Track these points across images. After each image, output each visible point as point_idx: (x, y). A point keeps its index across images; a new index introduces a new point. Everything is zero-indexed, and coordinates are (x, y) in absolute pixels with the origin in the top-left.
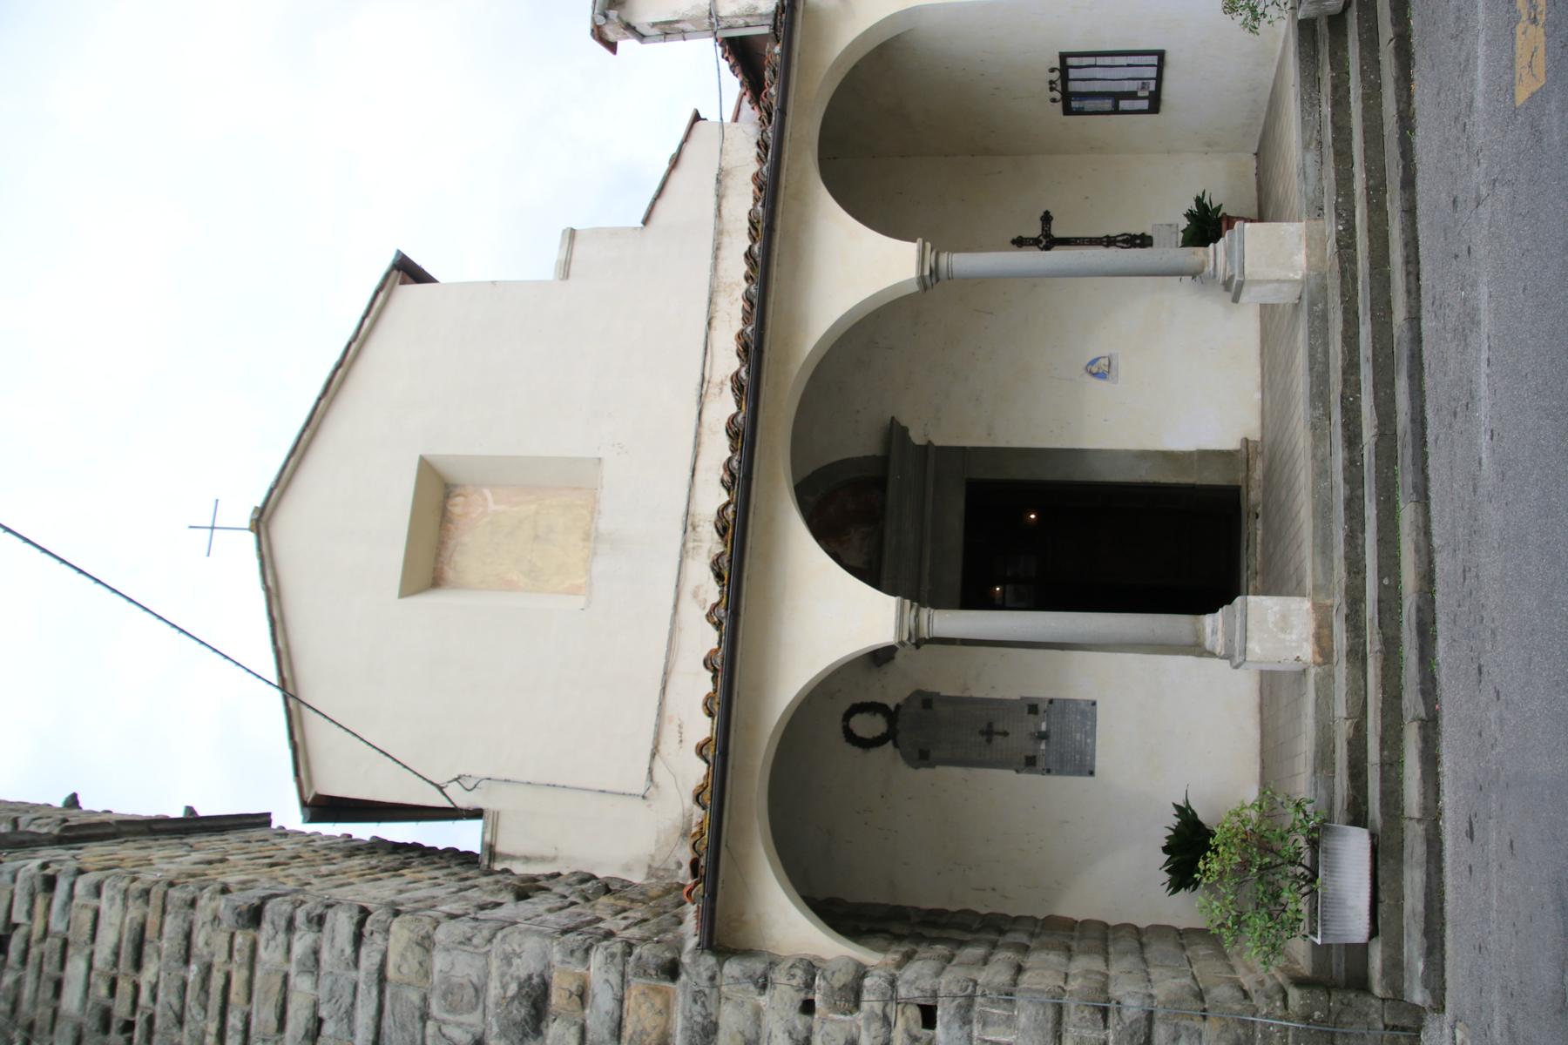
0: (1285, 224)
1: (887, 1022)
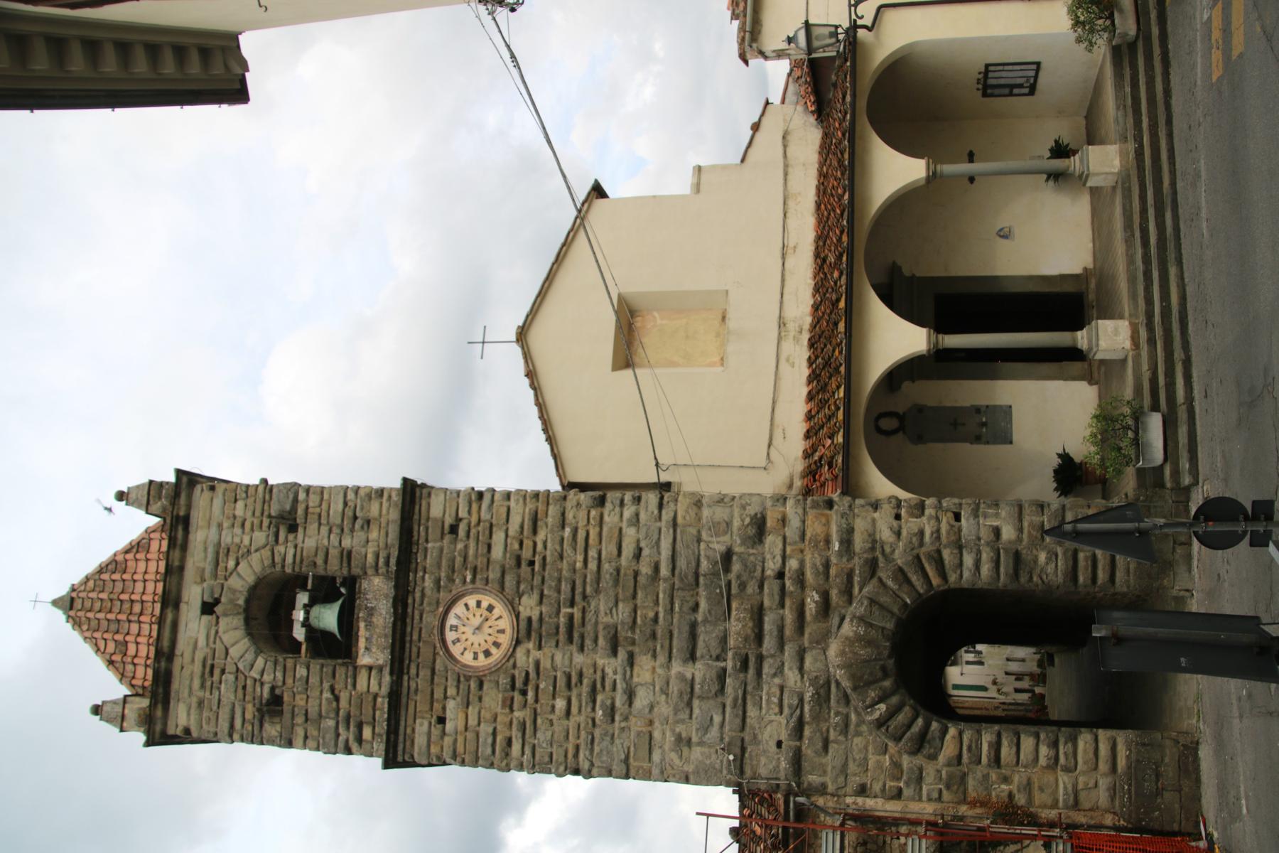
0: (1109, 146)
1: (938, 519)
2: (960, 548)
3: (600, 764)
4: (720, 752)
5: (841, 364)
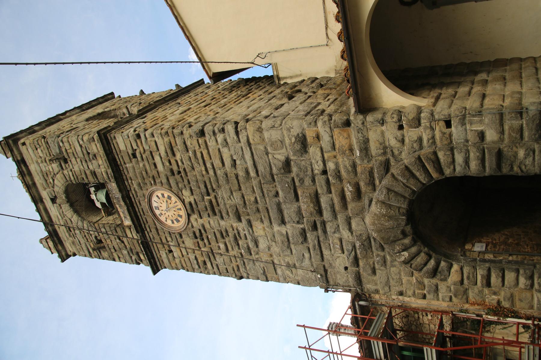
1: (432, 129)
2: (452, 150)
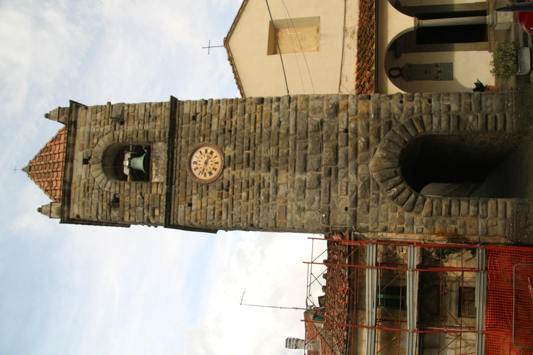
1: (420, 102)
2: (431, 115)
3: (263, 221)
4: (318, 213)
5: (373, 34)
